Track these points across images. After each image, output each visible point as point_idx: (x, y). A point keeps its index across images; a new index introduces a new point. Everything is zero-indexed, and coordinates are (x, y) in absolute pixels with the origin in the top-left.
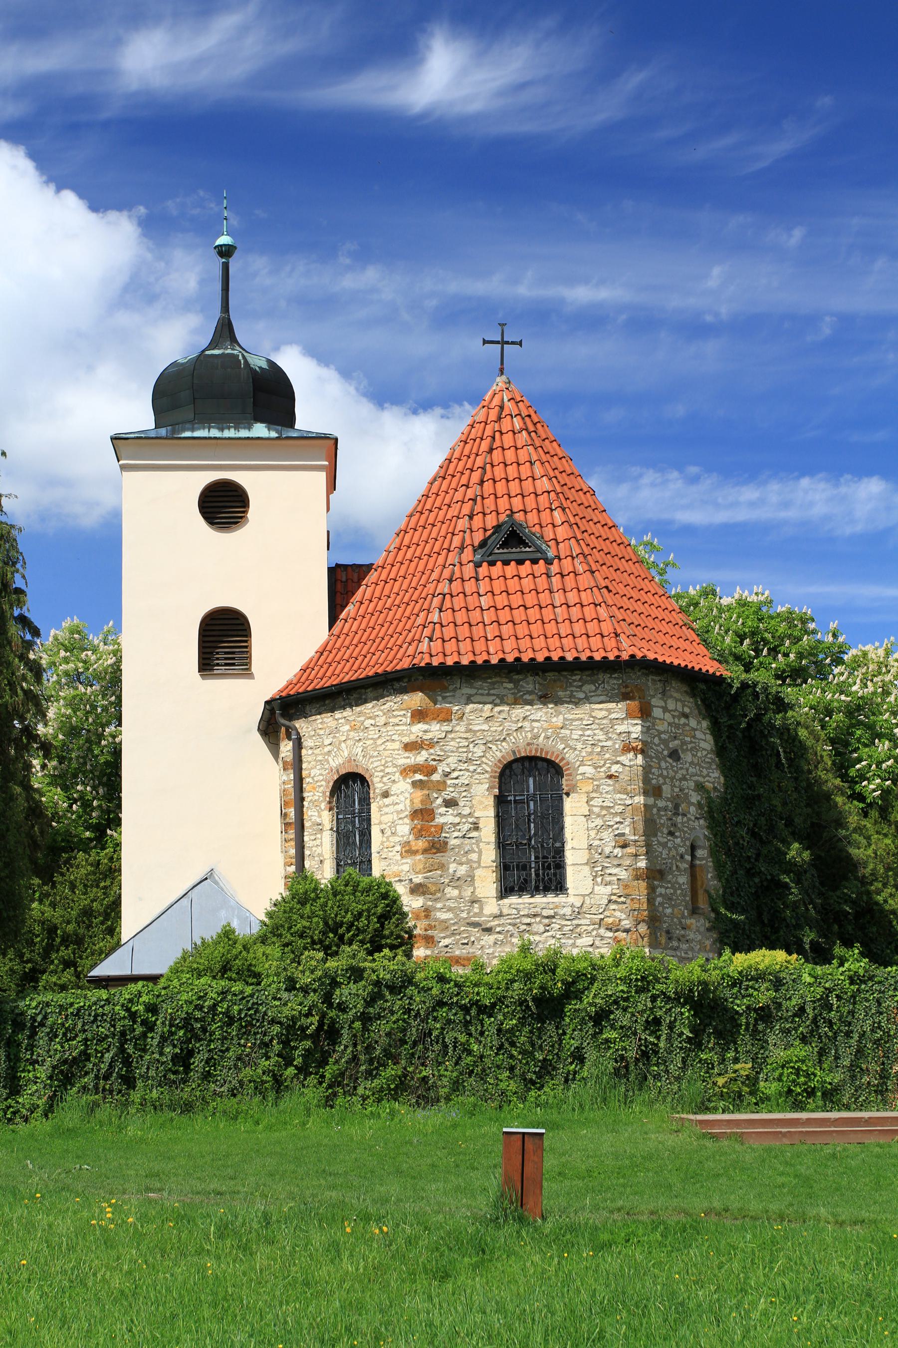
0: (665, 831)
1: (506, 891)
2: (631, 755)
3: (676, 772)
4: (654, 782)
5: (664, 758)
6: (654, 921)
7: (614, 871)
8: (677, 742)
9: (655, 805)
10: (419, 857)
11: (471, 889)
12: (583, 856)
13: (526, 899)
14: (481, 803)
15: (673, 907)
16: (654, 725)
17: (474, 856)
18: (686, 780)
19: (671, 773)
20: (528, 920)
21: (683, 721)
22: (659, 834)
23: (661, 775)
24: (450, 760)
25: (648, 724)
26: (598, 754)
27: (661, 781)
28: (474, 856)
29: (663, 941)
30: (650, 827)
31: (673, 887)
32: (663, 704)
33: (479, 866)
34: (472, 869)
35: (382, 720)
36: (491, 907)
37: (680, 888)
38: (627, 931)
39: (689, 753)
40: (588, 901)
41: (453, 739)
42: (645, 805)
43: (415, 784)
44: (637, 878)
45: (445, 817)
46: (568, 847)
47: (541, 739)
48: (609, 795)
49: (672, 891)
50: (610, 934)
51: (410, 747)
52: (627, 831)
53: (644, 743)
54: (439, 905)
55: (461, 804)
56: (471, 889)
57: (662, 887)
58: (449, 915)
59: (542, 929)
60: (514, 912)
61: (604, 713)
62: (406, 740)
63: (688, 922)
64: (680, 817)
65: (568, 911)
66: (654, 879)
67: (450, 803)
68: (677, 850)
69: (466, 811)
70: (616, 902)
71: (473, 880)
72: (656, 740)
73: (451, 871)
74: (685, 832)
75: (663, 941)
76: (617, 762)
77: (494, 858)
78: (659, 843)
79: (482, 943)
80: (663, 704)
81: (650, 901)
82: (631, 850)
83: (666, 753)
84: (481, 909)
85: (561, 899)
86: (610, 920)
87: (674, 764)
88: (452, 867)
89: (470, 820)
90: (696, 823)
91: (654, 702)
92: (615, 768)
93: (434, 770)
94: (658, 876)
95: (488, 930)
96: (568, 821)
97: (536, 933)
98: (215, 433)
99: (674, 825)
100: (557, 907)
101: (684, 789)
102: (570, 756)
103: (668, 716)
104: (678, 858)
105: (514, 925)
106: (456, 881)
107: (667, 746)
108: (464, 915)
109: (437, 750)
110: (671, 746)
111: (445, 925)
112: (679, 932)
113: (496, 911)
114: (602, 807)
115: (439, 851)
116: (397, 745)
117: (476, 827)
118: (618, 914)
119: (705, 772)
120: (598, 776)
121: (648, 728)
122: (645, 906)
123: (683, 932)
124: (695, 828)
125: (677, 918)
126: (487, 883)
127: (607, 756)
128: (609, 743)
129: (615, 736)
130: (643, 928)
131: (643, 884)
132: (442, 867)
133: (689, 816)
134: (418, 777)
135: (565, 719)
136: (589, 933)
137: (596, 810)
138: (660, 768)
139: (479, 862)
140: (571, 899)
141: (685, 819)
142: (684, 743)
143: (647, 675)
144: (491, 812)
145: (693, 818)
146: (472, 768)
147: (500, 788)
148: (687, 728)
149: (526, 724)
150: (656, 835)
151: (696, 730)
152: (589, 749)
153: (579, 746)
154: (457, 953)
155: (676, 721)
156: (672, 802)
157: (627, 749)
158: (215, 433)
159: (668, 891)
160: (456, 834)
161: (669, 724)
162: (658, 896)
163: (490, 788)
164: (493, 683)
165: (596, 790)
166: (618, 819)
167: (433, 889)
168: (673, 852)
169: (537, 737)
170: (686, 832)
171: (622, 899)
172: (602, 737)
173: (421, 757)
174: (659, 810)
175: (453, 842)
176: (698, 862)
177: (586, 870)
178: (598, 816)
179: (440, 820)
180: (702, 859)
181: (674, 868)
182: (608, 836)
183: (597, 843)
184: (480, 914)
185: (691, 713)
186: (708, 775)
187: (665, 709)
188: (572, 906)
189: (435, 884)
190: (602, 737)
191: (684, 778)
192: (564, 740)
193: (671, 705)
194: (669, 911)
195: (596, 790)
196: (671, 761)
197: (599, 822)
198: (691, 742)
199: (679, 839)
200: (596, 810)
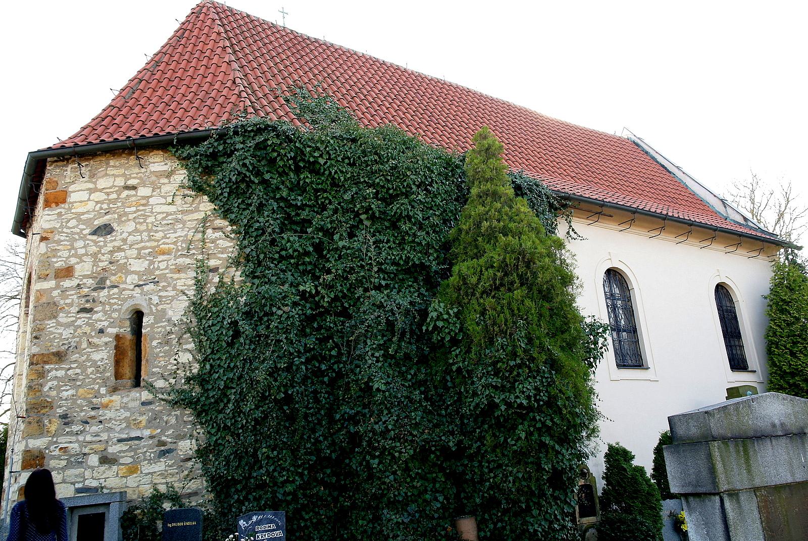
0: (75, 309)
3: (101, 247)
5: (84, 238)
8: (107, 217)
16: (70, 209)
18: (124, 250)
19: (94, 249)
21: (126, 192)
22: (61, 315)
25: (59, 210)
27: (73, 261)
32: (91, 186)
49: (78, 371)
57: (56, 370)
63: (105, 400)
64: (106, 290)
66: (46, 363)
72: (73, 223)
78: (59, 324)
80: (91, 186)
83: (87, 231)
87: (101, 239)
90: (138, 290)
94: (54, 359)
101: (118, 261)
104: (93, 334)
110: (96, 223)
123: (93, 413)
124: (132, 297)
125: (84, 399)
133: (122, 286)
138: (73, 248)
141: (116, 290)
143: (66, 166)
145: (132, 287)
148: (134, 199)
150: (55, 317)
151: (151, 196)
156: (93, 278)
159: (70, 372)
162: (50, 380)
170: (115, 304)
181: (84, 345)
186: (165, 237)
191: (119, 249)
193: (102, 183)
196: (94, 237)
198: (135, 212)
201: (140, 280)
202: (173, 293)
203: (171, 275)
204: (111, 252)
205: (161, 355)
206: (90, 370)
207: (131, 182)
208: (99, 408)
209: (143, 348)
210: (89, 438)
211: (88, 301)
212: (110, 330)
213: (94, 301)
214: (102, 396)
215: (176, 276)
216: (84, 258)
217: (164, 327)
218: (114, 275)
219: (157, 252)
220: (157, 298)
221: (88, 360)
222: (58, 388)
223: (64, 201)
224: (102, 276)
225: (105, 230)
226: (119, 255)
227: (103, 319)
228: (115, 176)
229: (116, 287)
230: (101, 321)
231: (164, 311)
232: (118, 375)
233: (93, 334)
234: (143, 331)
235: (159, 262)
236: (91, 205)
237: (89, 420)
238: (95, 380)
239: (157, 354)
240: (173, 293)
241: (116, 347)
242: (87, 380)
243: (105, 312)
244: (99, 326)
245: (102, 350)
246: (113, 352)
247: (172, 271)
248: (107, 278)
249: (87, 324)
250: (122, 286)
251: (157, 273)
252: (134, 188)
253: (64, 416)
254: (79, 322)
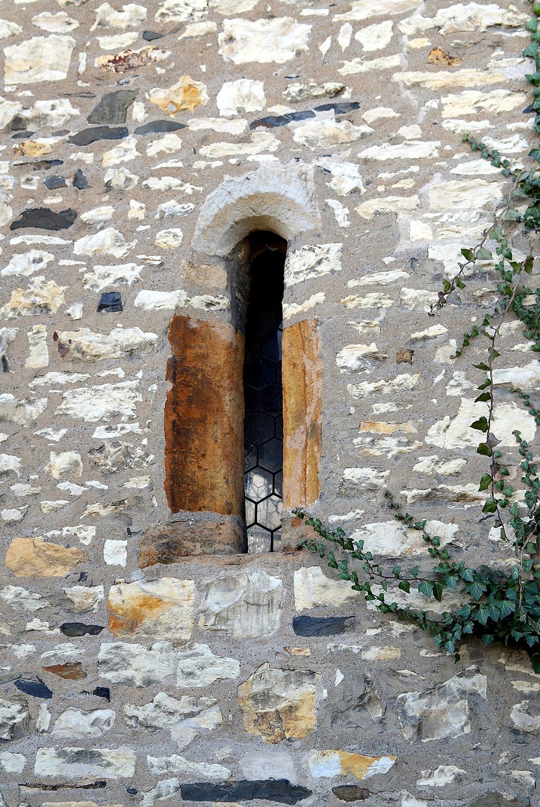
63: (126, 595)
64: (130, 142)
101: (179, 28)
104: (76, 311)
123: (69, 650)
124: (242, 166)
125: (34, 582)
133: (197, 125)
141: (171, 141)
145: (239, 127)
170: (169, 193)
181: (39, 356)
199: (104, 239)
201: (272, 99)
202: (425, 149)
203: (411, 77)
205: (382, 407)
206: (60, 462)
208: (95, 630)
209: (289, 378)
210: (47, 765)
211: (54, 184)
212: (150, 299)
213: (79, 181)
214: (113, 576)
215: (437, 78)
216: (42, 20)
217: (392, 290)
218: (164, 82)
220: (352, 169)
221: (53, 418)
224: (112, 88)
227: (119, 253)
229: (172, 127)
230: (110, 260)
231: (386, 223)
232: (181, 491)
233: (76, 311)
234: (289, 310)
235: (358, 25)
237: (51, 681)
238: (80, 503)
239: (363, 406)
240: (425, 149)
241: (177, 370)
242: (47, 505)
243: (127, 228)
244: (102, 279)
245: (114, 379)
246: (160, 388)
247: (417, 60)
248: (133, 96)
249: (52, 272)
250: (197, 125)
251: (351, 67)
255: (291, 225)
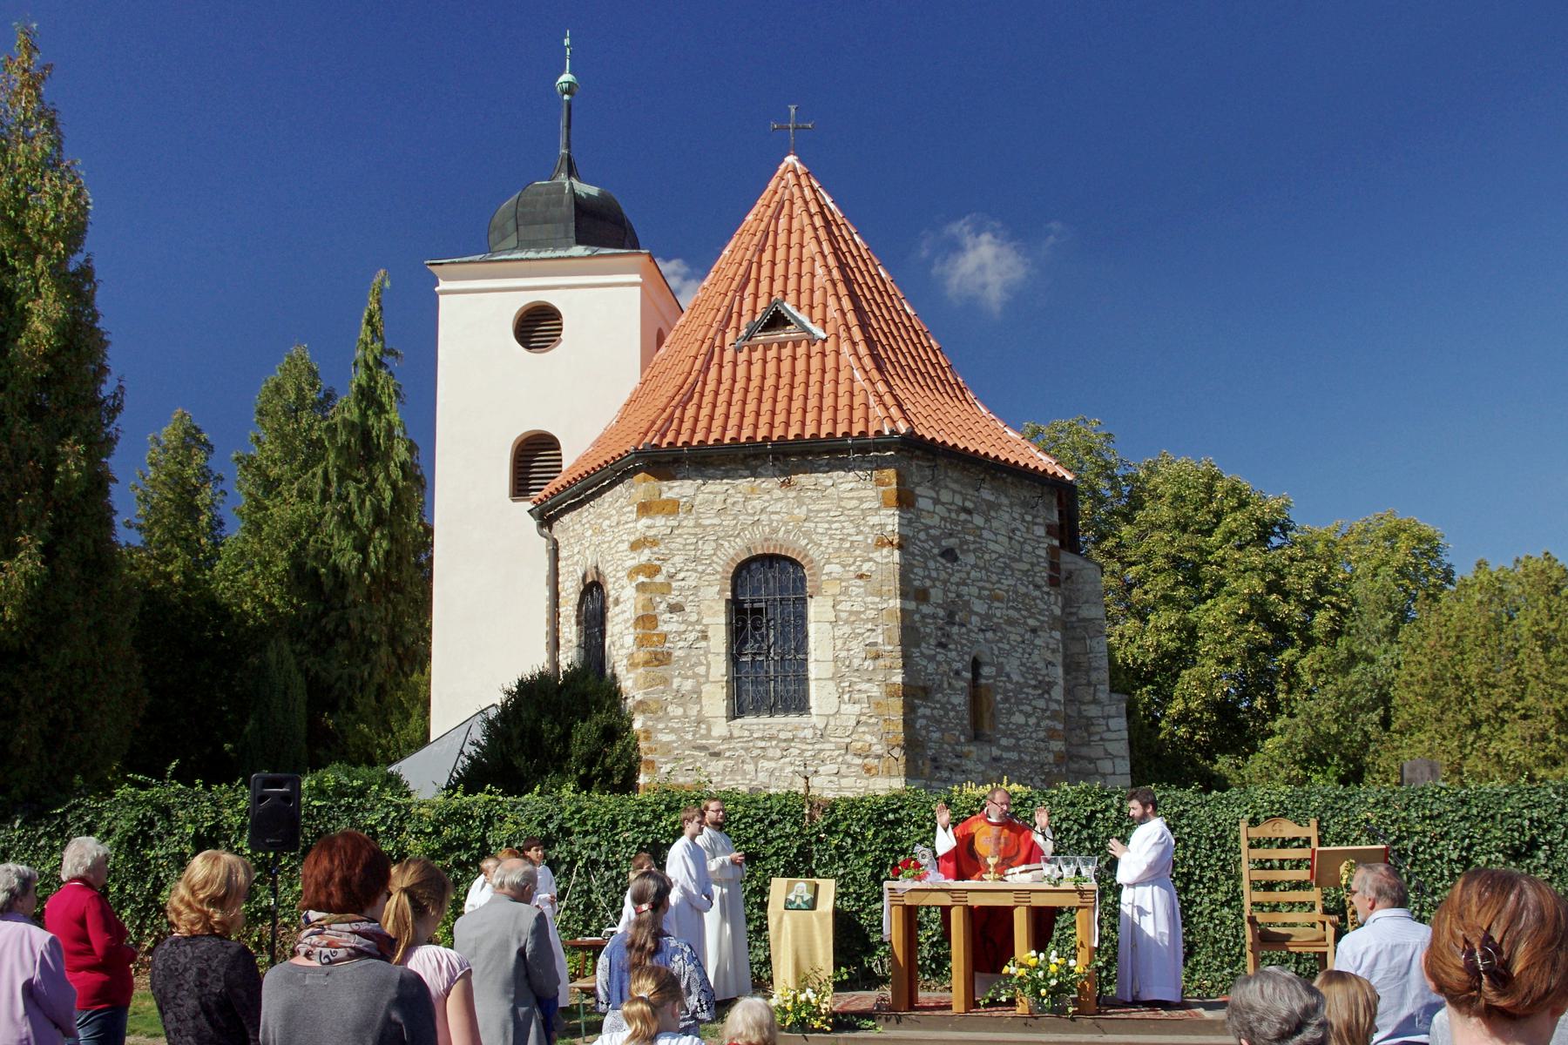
0: (933, 642)
1: (737, 710)
2: (885, 551)
3: (951, 575)
4: (917, 583)
5: (934, 558)
6: (913, 746)
7: (865, 686)
9: (918, 611)
10: (641, 670)
11: (697, 707)
12: (827, 670)
13: (764, 719)
14: (710, 607)
15: (943, 731)
16: (918, 517)
17: (701, 670)
19: (943, 575)
20: (763, 744)
21: (963, 516)
23: (929, 577)
24: (676, 559)
26: (847, 550)
27: (928, 583)
28: (701, 670)
29: (927, 771)
30: (910, 635)
31: (943, 707)
33: (708, 681)
34: (699, 684)
35: (615, 519)
36: (720, 728)
37: (954, 709)
38: (879, 757)
39: (972, 556)
40: (832, 722)
41: (680, 535)
42: (902, 610)
43: (641, 587)
44: (890, 695)
45: (669, 624)
46: (811, 658)
47: (781, 533)
48: (859, 599)
50: (858, 761)
51: (635, 546)
52: (880, 640)
53: (901, 536)
54: (661, 726)
55: (688, 609)
56: (697, 707)
58: (672, 737)
59: (778, 753)
60: (746, 733)
61: (854, 503)
62: (632, 538)
63: (966, 749)
65: (809, 733)
66: (914, 696)
67: (675, 608)
68: (949, 664)
69: (694, 618)
70: (866, 724)
71: (700, 697)
72: (922, 536)
73: (675, 686)
74: (963, 645)
75: (927, 771)
76: (870, 560)
77: (724, 671)
79: (710, 769)
81: (908, 723)
82: (881, 662)
83: (936, 551)
84: (709, 730)
85: (804, 719)
86: (859, 745)
88: (676, 682)
89: (698, 628)
90: (981, 636)
91: (918, 490)
92: (866, 567)
93: (658, 570)
95: (717, 755)
96: (812, 628)
97: (772, 759)
98: (531, 255)
99: (948, 636)
100: (796, 729)
102: (814, 553)
103: (939, 508)
105: (746, 749)
106: (681, 698)
107: (940, 546)
108: (689, 737)
109: (662, 548)
110: (943, 543)
111: (667, 749)
112: (951, 761)
113: (725, 733)
114: (851, 613)
115: (661, 663)
116: (626, 546)
117: (705, 638)
118: (868, 737)
119: (994, 578)
120: (846, 576)
121: (910, 521)
122: (901, 728)
126: (716, 700)
127: (858, 552)
128: (860, 538)
129: (867, 530)
130: (897, 752)
131: (897, 703)
132: (666, 681)
134: (641, 579)
135: (809, 511)
136: (833, 760)
137: (844, 615)
138: (926, 568)
139: (707, 676)
140: (814, 719)
141: (964, 630)
142: (963, 542)
143: (911, 458)
144: (722, 619)
146: (700, 568)
147: (734, 591)
149: (763, 517)
150: (918, 646)
152: (836, 545)
153: (826, 541)
154: (681, 780)
155: (953, 515)
157: (881, 543)
158: (531, 255)
160: (681, 644)
161: (942, 518)
163: (721, 592)
164: (727, 471)
165: (845, 592)
166: (870, 626)
167: (654, 706)
168: (945, 667)
169: (775, 531)
171: (873, 720)
172: (852, 531)
173: (645, 556)
174: (924, 616)
175: (677, 653)
176: (983, 681)
177: (831, 686)
178: (846, 622)
179: (663, 628)
180: (987, 678)
182: (857, 647)
183: (843, 654)
184: (708, 736)
185: (976, 508)
186: (999, 582)
187: (936, 501)
188: (814, 727)
189: (657, 701)
190: (852, 531)
192: (806, 534)
193: (945, 496)
194: (936, 736)
195: (845, 592)
197: (847, 629)
200: (844, 615)
204: (958, 584)
207: (969, 505)
219: (994, 598)
222: (926, 727)
223: (913, 506)
225: (949, 555)
226: (964, 590)
228: (954, 492)
234: (983, 681)
236: (936, 520)
252: (969, 512)
253: (934, 760)
254: (939, 658)
255: (985, 658)
